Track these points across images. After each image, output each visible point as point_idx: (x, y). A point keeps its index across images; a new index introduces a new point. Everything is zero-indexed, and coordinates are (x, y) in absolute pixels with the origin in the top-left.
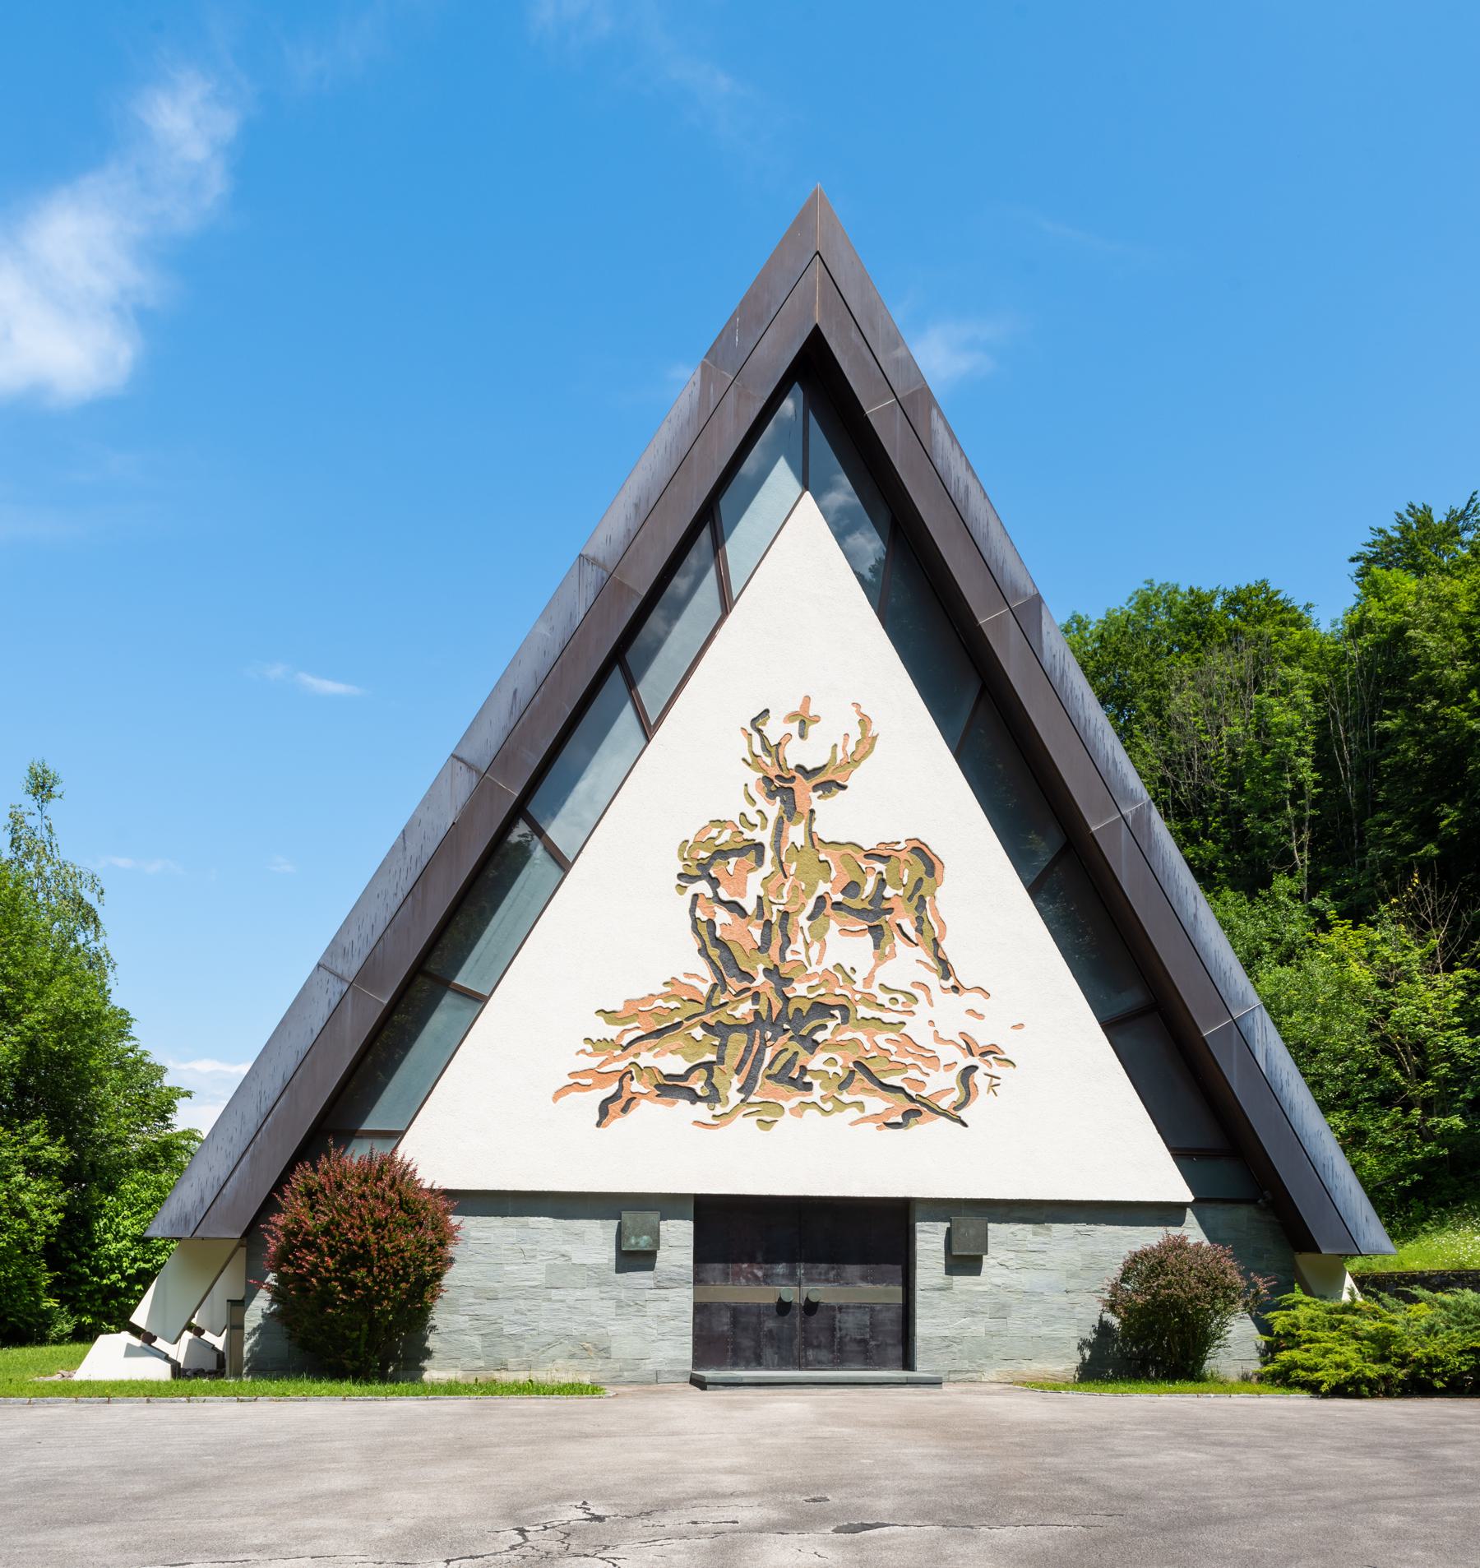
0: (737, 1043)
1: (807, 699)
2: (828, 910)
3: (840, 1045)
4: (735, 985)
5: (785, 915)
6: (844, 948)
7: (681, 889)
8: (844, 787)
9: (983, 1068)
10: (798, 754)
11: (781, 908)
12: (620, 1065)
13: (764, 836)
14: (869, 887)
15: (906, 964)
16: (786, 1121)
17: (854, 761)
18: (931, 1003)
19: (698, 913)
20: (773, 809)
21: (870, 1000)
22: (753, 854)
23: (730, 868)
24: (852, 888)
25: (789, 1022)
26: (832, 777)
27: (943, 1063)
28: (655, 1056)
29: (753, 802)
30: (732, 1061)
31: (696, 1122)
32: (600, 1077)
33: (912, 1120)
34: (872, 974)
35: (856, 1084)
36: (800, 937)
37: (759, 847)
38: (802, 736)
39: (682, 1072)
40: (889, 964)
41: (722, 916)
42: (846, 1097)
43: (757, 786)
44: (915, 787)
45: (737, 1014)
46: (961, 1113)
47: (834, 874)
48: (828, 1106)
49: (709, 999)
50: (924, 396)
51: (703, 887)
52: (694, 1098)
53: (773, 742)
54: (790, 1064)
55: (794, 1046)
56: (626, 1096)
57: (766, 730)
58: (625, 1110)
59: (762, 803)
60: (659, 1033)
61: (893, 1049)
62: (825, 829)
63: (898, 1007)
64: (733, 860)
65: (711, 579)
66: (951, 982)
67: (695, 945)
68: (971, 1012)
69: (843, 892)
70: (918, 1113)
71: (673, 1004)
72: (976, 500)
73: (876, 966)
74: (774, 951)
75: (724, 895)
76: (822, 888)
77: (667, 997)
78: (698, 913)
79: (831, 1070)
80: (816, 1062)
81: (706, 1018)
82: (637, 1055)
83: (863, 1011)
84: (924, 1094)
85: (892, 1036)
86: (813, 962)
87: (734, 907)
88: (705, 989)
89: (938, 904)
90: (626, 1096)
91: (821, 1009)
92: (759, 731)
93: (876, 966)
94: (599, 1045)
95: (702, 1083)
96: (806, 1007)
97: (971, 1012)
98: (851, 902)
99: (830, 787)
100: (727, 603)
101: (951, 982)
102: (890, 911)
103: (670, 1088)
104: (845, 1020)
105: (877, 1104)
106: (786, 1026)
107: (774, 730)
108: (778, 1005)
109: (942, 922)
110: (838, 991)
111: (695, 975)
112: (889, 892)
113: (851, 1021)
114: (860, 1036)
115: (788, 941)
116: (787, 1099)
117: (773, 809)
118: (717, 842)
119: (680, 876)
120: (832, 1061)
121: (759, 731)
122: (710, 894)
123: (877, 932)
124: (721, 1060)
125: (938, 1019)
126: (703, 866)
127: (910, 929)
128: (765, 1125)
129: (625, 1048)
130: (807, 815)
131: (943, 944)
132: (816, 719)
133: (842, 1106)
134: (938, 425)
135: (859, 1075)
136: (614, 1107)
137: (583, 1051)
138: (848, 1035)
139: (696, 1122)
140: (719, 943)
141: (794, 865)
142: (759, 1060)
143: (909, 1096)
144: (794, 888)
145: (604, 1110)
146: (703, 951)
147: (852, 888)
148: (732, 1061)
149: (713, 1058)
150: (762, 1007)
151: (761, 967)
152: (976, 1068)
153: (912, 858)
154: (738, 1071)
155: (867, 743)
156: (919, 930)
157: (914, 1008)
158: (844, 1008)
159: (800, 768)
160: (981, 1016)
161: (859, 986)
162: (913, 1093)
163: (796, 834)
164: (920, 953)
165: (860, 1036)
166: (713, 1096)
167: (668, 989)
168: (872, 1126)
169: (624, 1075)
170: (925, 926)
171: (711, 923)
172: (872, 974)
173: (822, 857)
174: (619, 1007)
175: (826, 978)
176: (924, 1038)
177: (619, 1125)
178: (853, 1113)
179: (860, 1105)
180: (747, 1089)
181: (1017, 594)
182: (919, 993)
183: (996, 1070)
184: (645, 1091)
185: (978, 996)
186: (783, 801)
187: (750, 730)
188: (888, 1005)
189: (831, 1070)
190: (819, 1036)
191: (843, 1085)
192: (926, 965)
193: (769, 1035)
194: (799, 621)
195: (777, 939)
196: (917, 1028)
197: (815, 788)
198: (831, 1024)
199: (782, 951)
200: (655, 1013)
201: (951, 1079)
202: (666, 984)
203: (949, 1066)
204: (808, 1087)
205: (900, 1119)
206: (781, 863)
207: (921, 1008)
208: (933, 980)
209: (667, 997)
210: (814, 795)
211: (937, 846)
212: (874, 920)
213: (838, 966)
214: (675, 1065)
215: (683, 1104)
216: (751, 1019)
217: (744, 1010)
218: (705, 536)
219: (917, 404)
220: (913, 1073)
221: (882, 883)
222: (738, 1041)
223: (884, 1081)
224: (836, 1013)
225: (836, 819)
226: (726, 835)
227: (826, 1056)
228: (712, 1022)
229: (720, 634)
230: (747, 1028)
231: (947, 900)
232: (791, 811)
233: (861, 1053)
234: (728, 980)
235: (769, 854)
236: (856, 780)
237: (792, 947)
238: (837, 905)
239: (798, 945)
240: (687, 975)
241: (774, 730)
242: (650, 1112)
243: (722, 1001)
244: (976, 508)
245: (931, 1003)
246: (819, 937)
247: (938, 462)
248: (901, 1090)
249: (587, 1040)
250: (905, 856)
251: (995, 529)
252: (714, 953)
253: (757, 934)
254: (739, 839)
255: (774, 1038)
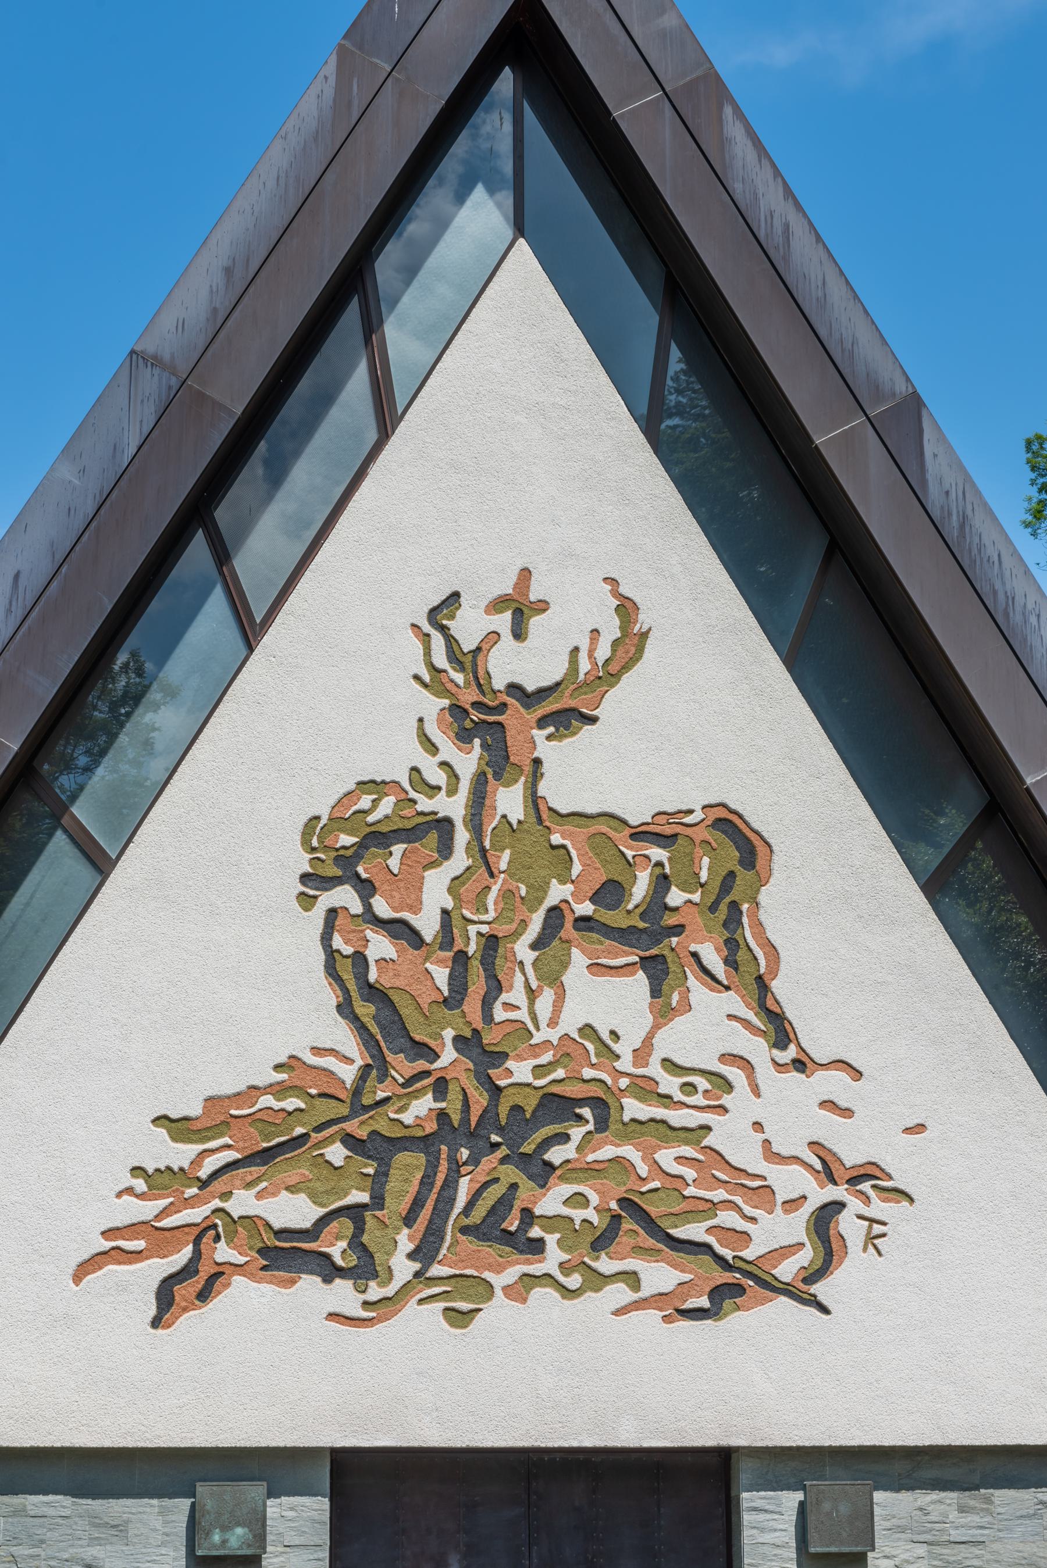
0: (407, 1171)
1: (526, 573)
2: (568, 930)
3: (593, 1171)
4: (402, 1066)
5: (491, 942)
6: (603, 998)
7: (306, 901)
8: (593, 720)
9: (855, 1205)
10: (510, 665)
11: (485, 929)
12: (195, 1215)
13: (454, 806)
14: (640, 889)
15: (710, 1024)
16: (497, 1312)
17: (609, 675)
18: (756, 1091)
19: (338, 942)
20: (468, 762)
21: (645, 1089)
22: (433, 837)
23: (394, 863)
24: (610, 893)
25: (501, 1130)
26: (572, 703)
27: (780, 1199)
28: (259, 1196)
29: (432, 748)
30: (398, 1203)
31: (333, 1316)
32: (158, 1237)
33: (727, 1304)
34: (648, 1042)
35: (624, 1240)
36: (519, 978)
37: (444, 825)
38: (519, 633)
39: (307, 1224)
40: (680, 1023)
41: (380, 947)
42: (605, 1265)
43: (440, 721)
44: (712, 713)
45: (408, 1118)
46: (819, 1289)
47: (577, 869)
48: (574, 1281)
49: (357, 1092)
50: (711, 87)
51: (345, 897)
52: (330, 1271)
53: (468, 644)
54: (504, 1204)
55: (510, 1173)
56: (205, 1270)
57: (455, 626)
58: (204, 1295)
59: (448, 750)
60: (265, 1156)
61: (690, 1174)
62: (560, 791)
63: (698, 1100)
64: (398, 849)
65: (358, 383)
66: (792, 1052)
67: (330, 997)
68: (828, 1105)
69: (595, 898)
70: (738, 1290)
71: (292, 1103)
72: (801, 245)
73: (656, 1027)
74: (472, 1006)
75: (382, 907)
76: (558, 892)
77: (280, 1090)
78: (338, 942)
79: (578, 1215)
80: (551, 1202)
81: (351, 1126)
82: (226, 1196)
83: (634, 1108)
84: (749, 1254)
85: (688, 1151)
86: (543, 1023)
87: (401, 930)
88: (348, 1074)
89: (763, 916)
90: (205, 1270)
91: (558, 1106)
92: (443, 629)
93: (656, 1027)
94: (159, 1180)
95: (343, 1244)
96: (530, 1104)
97: (828, 1105)
98: (609, 917)
99: (568, 720)
100: (387, 418)
101: (792, 1052)
102: (678, 930)
103: (285, 1255)
104: (602, 1124)
105: (660, 1276)
106: (495, 1138)
107: (470, 625)
108: (480, 1100)
109: (771, 949)
110: (588, 1073)
111: (332, 1052)
112: (675, 897)
113: (613, 1127)
114: (629, 1152)
115: (496, 987)
116: (499, 1269)
117: (468, 762)
118: (370, 819)
119: (305, 878)
120: (578, 1200)
121: (443, 629)
122: (356, 907)
123: (657, 970)
124: (378, 1200)
125: (770, 1118)
126: (347, 860)
127: (713, 958)
128: (459, 1318)
129: (204, 1184)
130: (528, 768)
131: (775, 985)
132: (542, 606)
133: (598, 1281)
134: (735, 131)
135: (628, 1224)
136: (184, 1291)
137: (129, 1191)
138: (608, 1152)
139: (333, 1316)
140: (374, 993)
141: (506, 855)
142: (446, 1200)
143: (720, 1259)
144: (507, 894)
145: (166, 1301)
146: (345, 1009)
147: (610, 893)
148: (398, 1203)
149: (360, 1197)
150: (453, 1105)
151: (449, 1034)
152: (841, 1205)
153: (715, 837)
154: (409, 1221)
155: (632, 644)
156: (731, 962)
157: (726, 1100)
158: (599, 1105)
159: (514, 689)
160: (847, 1113)
161: (625, 1064)
162: (727, 1254)
163: (509, 801)
164: (734, 1002)
165: (629, 1152)
166: (365, 1268)
167: (284, 1076)
168: (653, 1316)
169: (202, 1234)
170: (742, 955)
171: (360, 959)
172: (648, 1042)
173: (556, 839)
174: (195, 1109)
175: (567, 1051)
176: (745, 1154)
177: (192, 1324)
178: (619, 1294)
179: (632, 1279)
180: (424, 1252)
181: (878, 393)
182: (735, 1074)
183: (878, 1208)
184: (242, 1260)
185: (841, 1076)
186: (485, 746)
187: (427, 628)
188: (679, 1096)
189: (578, 1215)
190: (556, 1155)
191: (602, 1242)
192: (746, 1023)
193: (464, 1153)
194: (510, 445)
195: (477, 985)
196: (733, 1138)
197: (542, 723)
198: (577, 1133)
199: (487, 1005)
200: (261, 1120)
201: (794, 1227)
202: (278, 1067)
203: (792, 1204)
204: (537, 1247)
205: (704, 1302)
206: (483, 851)
207: (740, 1099)
208: (757, 1049)
209: (280, 1090)
210: (539, 735)
211: (759, 815)
212: (651, 947)
213: (588, 1030)
214: (293, 1210)
215: (309, 1283)
216: (431, 1127)
217: (421, 1108)
218: (352, 312)
219: (698, 100)
220: (727, 1218)
221: (662, 882)
222: (408, 1166)
223: (678, 1233)
224: (586, 1112)
225: (580, 773)
226: (386, 806)
227: (567, 1189)
228: (362, 1133)
229: (375, 471)
230: (425, 1143)
231: (781, 908)
232: (499, 764)
233: (632, 1183)
234: (390, 1057)
235: (462, 836)
236: (612, 706)
237: (504, 997)
238: (584, 922)
239: (516, 995)
240: (316, 1051)
241: (470, 625)
242: (249, 1300)
243: (381, 1095)
244: (803, 259)
245: (756, 1091)
246: (552, 975)
247: (737, 188)
248: (707, 1248)
249: (137, 1171)
250: (701, 834)
251: (836, 293)
252: (365, 1010)
253: (441, 975)
254: (407, 812)
255: (474, 1160)
